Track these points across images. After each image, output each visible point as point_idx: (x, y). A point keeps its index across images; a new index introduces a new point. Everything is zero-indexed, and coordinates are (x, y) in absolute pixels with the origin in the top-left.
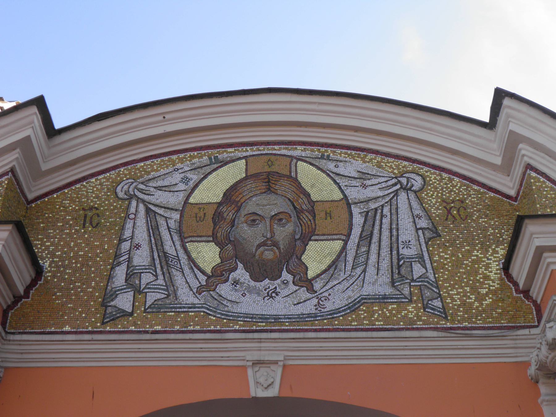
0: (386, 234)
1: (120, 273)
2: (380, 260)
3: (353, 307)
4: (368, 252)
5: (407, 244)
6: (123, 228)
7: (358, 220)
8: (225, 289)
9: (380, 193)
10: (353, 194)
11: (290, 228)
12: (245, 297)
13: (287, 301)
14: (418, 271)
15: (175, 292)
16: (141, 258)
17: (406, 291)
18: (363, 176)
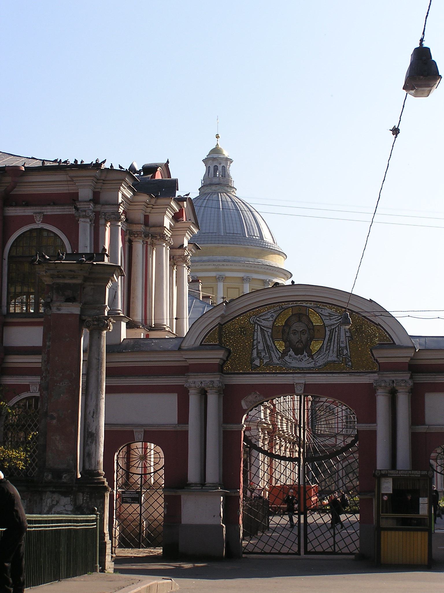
0: (336, 338)
1: (255, 352)
2: (334, 347)
4: (330, 345)
5: (342, 342)
6: (254, 335)
7: (328, 333)
8: (287, 358)
9: (336, 322)
10: (327, 322)
11: (306, 336)
12: (293, 361)
13: (305, 363)
14: (345, 352)
15: (272, 359)
16: (261, 347)
17: (341, 359)
18: (330, 315)
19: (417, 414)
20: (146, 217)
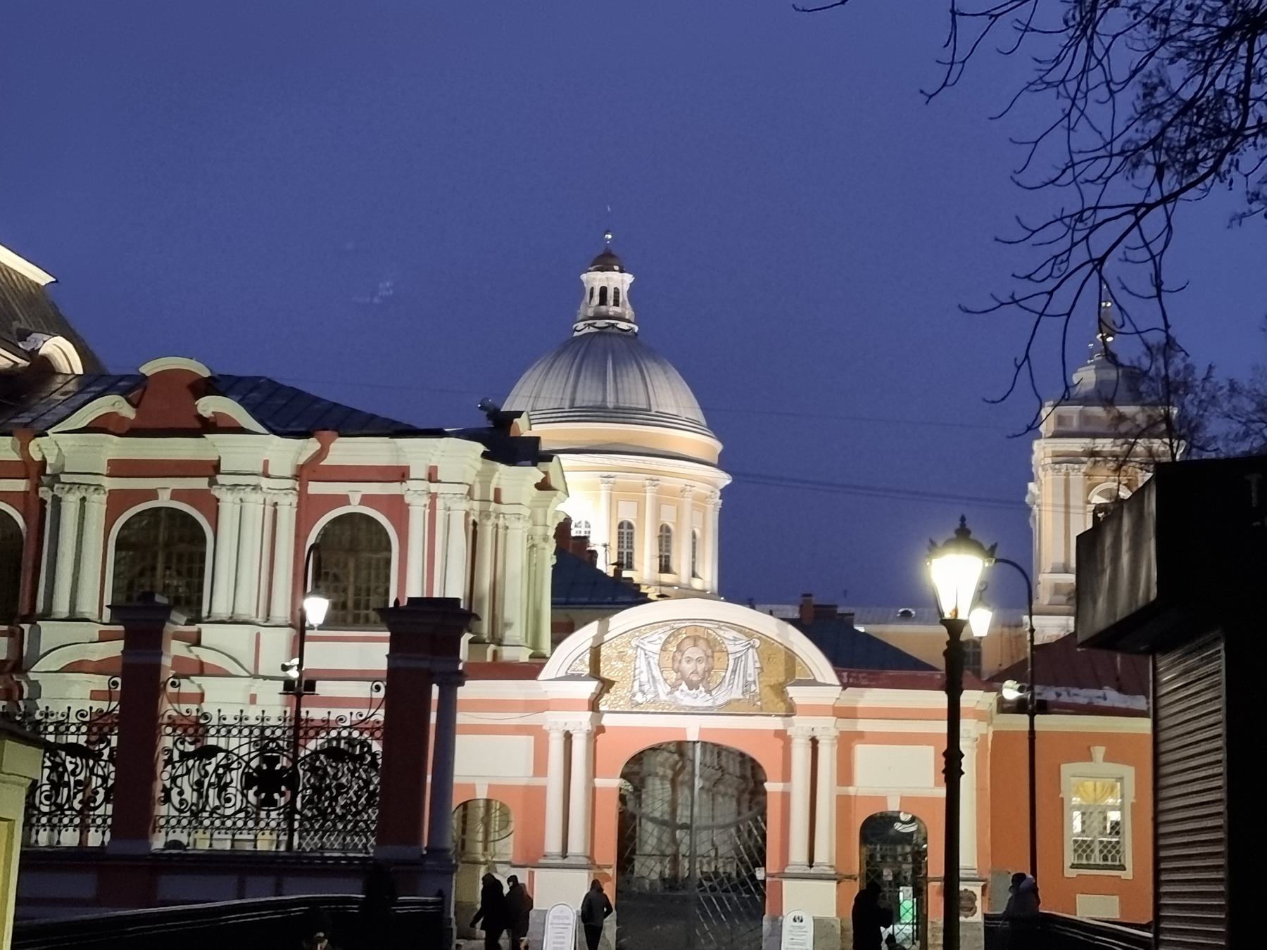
1: (636, 684)
3: (728, 703)
7: (731, 662)
8: (677, 693)
11: (703, 665)
13: (701, 699)
14: (753, 688)
16: (644, 678)
18: (735, 639)
19: (845, 773)
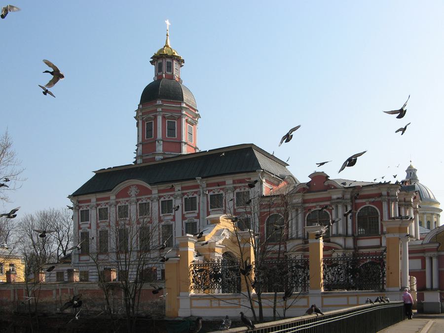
20: (405, 199)
